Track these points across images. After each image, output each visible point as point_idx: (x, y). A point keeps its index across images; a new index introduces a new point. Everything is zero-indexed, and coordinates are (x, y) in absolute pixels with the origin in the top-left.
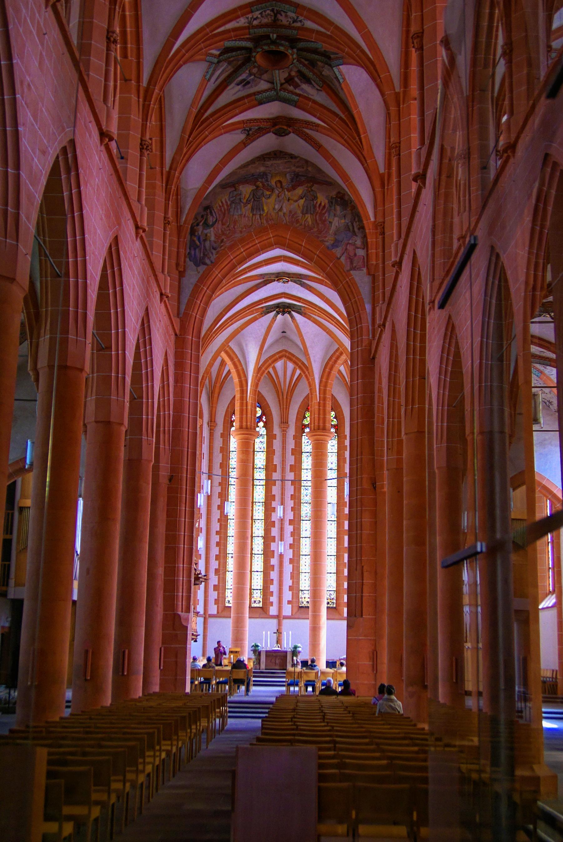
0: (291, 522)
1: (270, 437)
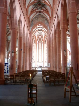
1: (39, 44)
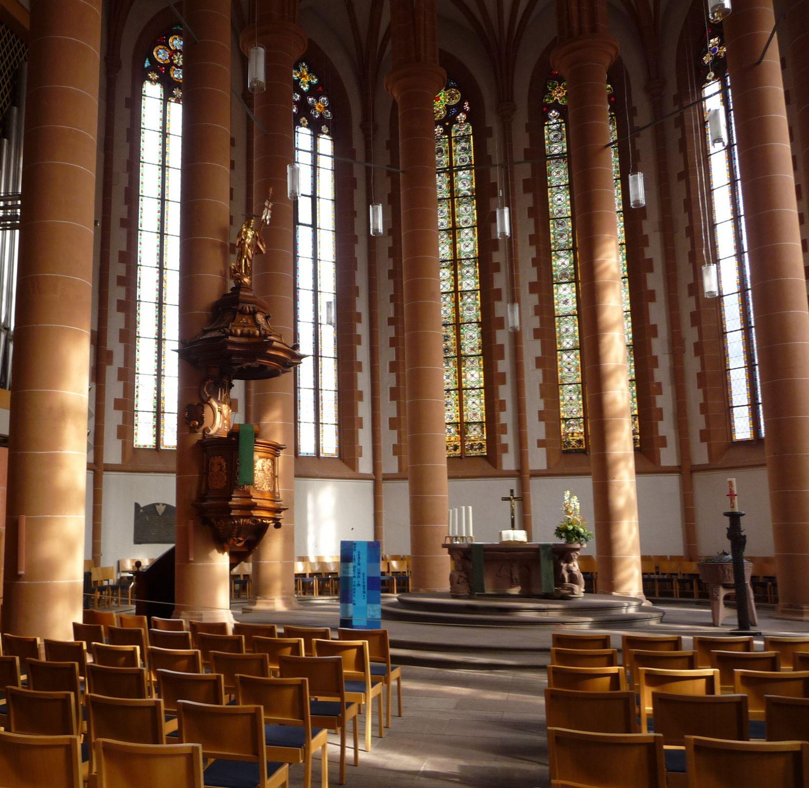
0: (533, 288)
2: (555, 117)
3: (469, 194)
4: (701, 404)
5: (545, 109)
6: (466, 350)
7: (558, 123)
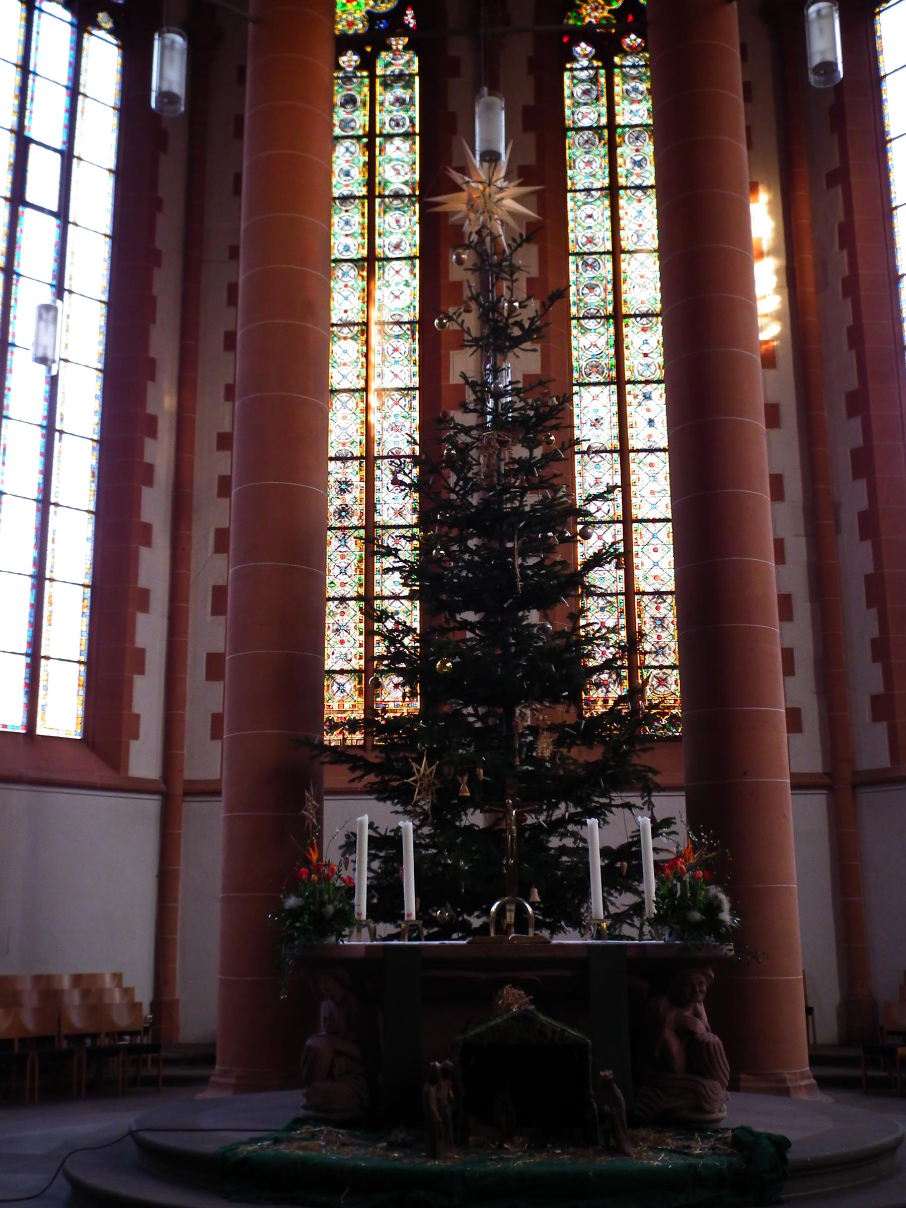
2: (586, 56)
3: (407, 191)
4: (873, 641)
5: (565, 40)
6: (385, 514)
7: (593, 68)
